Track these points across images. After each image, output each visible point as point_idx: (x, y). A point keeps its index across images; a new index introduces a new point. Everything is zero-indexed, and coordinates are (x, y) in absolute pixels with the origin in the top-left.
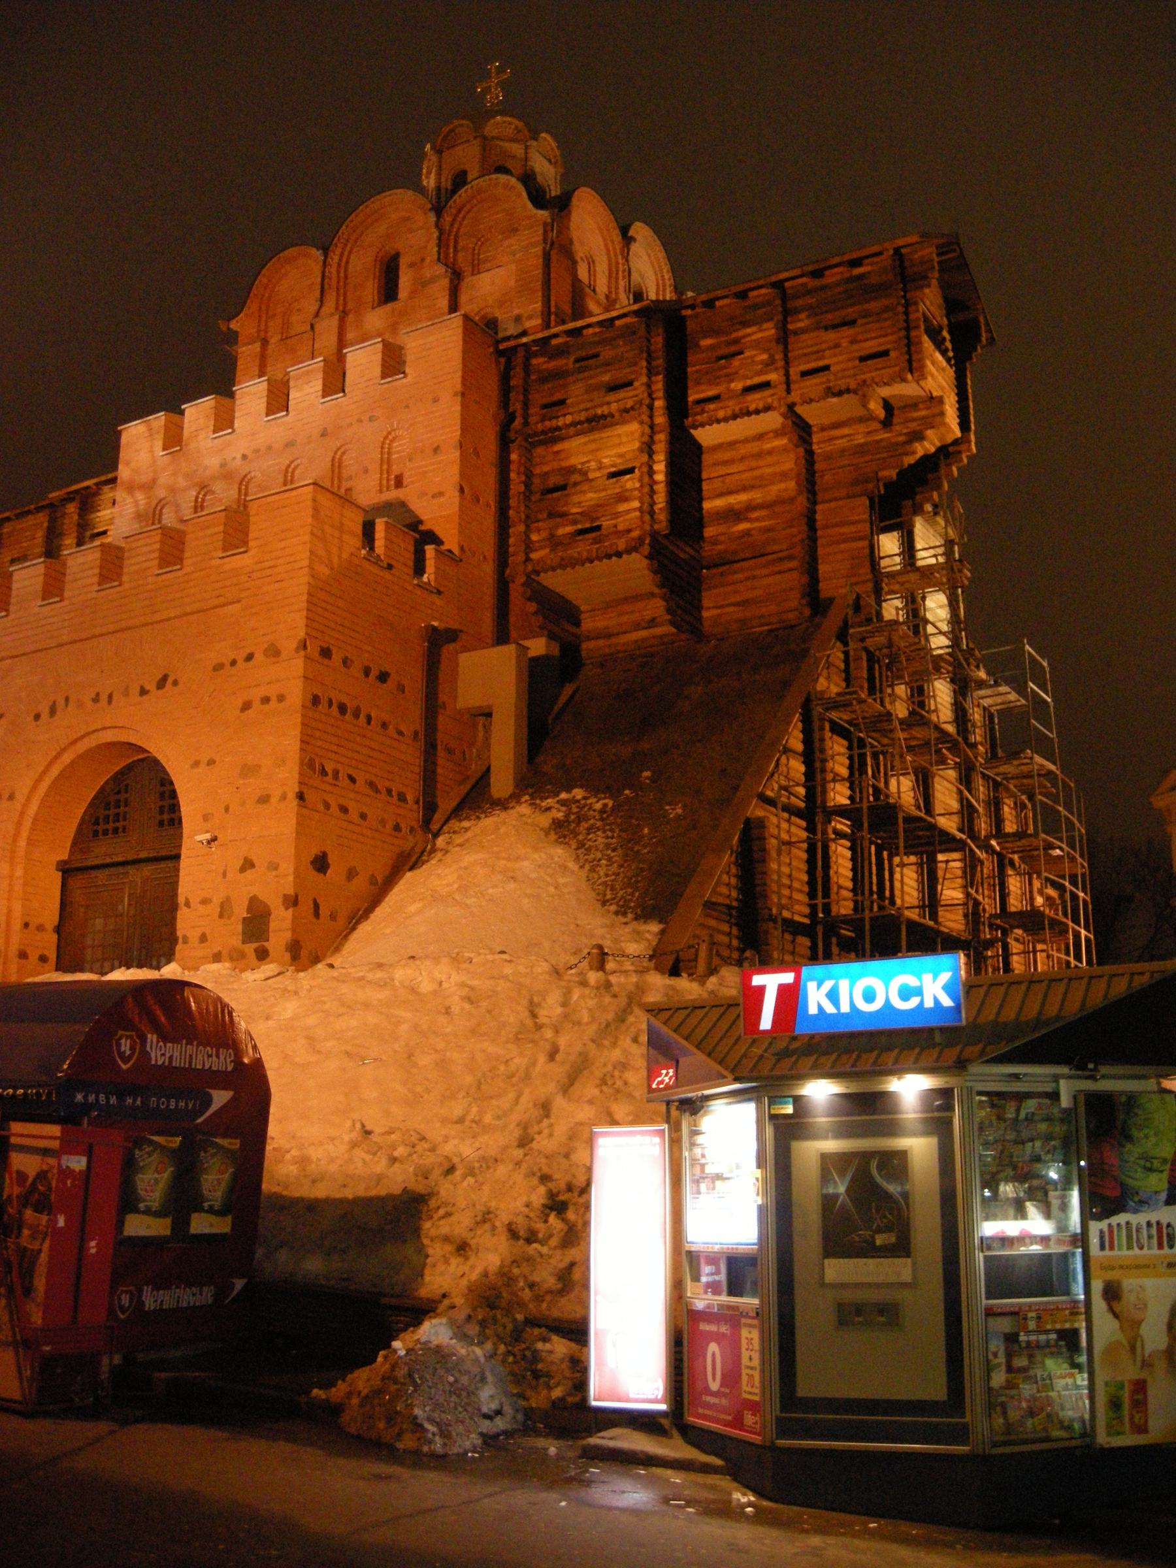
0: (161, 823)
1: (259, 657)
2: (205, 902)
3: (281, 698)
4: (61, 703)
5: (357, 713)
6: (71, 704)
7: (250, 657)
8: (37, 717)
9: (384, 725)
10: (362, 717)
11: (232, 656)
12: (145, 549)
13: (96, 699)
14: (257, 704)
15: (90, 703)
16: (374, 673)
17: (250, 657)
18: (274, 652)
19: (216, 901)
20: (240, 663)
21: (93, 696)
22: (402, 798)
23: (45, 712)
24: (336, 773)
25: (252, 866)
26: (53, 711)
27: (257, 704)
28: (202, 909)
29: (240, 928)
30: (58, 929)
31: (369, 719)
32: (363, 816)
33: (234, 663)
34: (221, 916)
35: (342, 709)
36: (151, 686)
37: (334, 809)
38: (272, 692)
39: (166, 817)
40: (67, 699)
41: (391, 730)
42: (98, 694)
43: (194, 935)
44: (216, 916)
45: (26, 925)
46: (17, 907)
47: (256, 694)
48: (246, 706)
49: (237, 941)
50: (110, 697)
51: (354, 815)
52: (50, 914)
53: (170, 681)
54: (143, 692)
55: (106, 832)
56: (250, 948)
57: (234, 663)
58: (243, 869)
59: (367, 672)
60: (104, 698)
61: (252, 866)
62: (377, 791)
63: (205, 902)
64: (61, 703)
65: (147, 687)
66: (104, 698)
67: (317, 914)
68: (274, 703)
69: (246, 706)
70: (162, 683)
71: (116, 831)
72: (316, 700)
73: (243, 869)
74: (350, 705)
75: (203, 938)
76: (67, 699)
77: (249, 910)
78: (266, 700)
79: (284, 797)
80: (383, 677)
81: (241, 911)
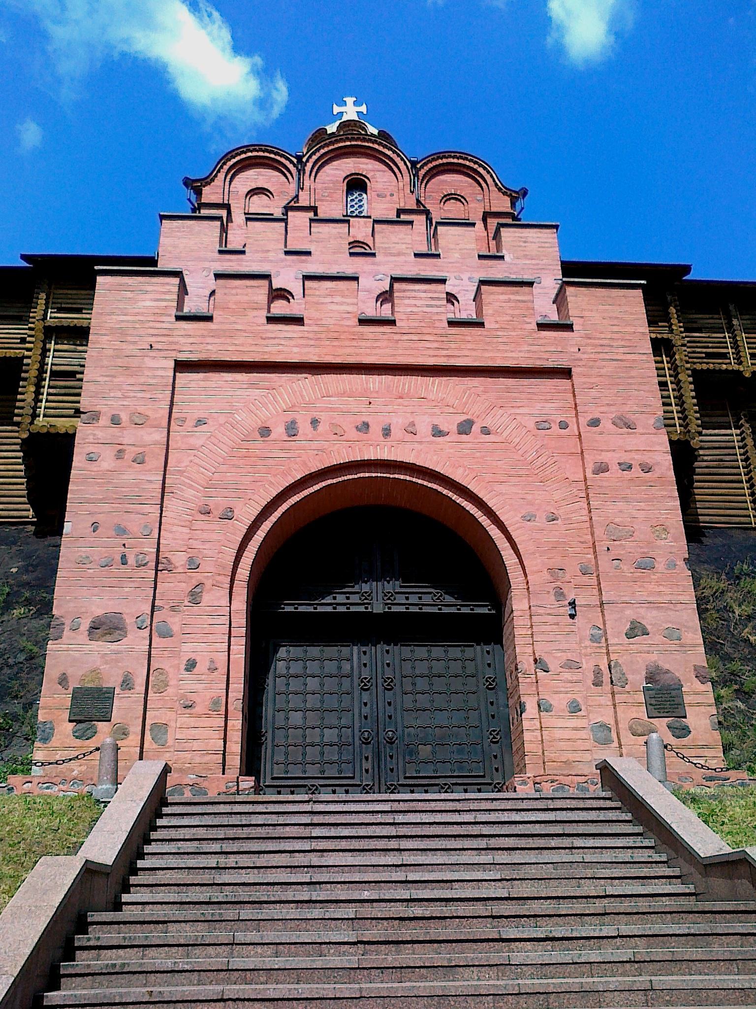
1: (606, 424)
2: (572, 665)
6: (320, 428)
8: (265, 432)
12: (423, 295)
14: (614, 467)
15: (353, 434)
17: (595, 423)
19: (588, 665)
21: (359, 424)
23: (279, 431)
25: (646, 633)
26: (292, 429)
27: (614, 467)
28: (567, 675)
38: (636, 459)
40: (315, 422)
42: (366, 425)
43: (559, 702)
44: (590, 683)
50: (387, 432)
53: (476, 428)
56: (661, 724)
60: (376, 430)
63: (572, 665)
64: (304, 427)
65: (444, 428)
66: (376, 430)
68: (636, 472)
69: (601, 469)
70: (465, 428)
75: (575, 708)
76: (315, 422)
77: (650, 679)
79: (672, 565)
81: (638, 679)
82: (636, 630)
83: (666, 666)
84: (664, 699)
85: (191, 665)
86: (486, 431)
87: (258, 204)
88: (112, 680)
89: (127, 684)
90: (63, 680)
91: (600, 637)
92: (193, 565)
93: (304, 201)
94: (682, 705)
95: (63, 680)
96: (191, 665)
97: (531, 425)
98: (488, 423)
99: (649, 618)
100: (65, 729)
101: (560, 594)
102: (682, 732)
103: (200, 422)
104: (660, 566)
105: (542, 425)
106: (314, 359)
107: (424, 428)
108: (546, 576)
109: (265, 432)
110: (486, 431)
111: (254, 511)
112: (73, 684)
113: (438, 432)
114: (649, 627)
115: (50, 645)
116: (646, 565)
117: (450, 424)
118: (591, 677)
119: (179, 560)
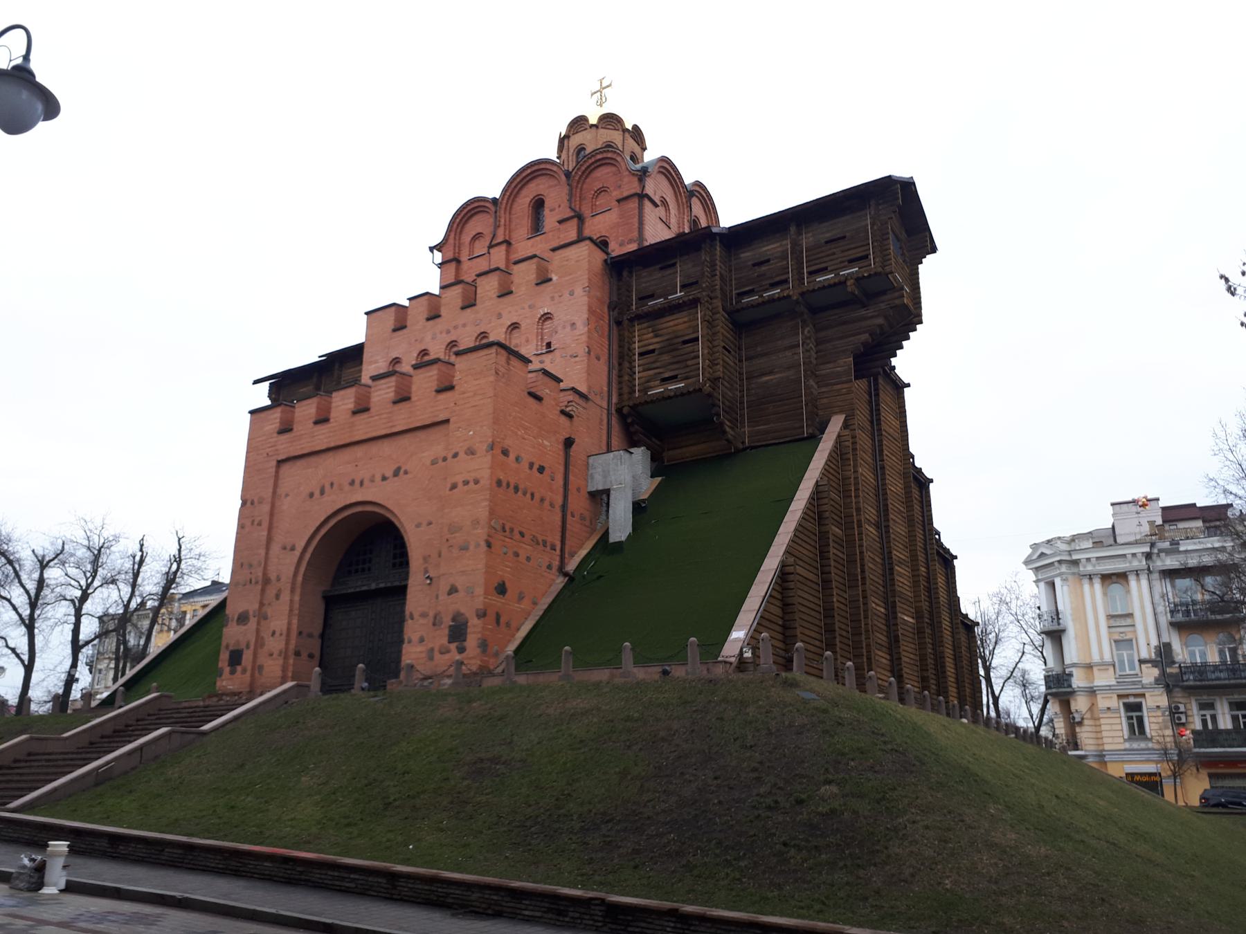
0: (394, 565)
1: (462, 455)
2: (424, 615)
3: (476, 482)
4: (327, 486)
5: (525, 494)
7: (456, 455)
8: (311, 495)
9: (542, 500)
10: (528, 495)
11: (443, 454)
13: (352, 483)
14: (460, 485)
15: (347, 487)
16: (536, 467)
17: (456, 455)
18: (471, 452)
19: (432, 614)
20: (449, 459)
22: (553, 548)
23: (317, 493)
24: (512, 530)
25: (457, 591)
26: (322, 492)
28: (422, 621)
29: (447, 632)
30: (322, 636)
31: (532, 495)
32: (528, 559)
33: (445, 459)
34: (434, 624)
35: (516, 489)
36: (389, 473)
37: (510, 554)
38: (470, 477)
39: (397, 561)
40: (332, 484)
41: (547, 503)
45: (300, 633)
46: (295, 621)
47: (459, 479)
48: (454, 487)
49: (445, 640)
50: (362, 483)
51: (522, 558)
52: (317, 628)
54: (384, 478)
55: (357, 571)
56: (453, 646)
57: (445, 459)
58: (450, 593)
59: (531, 465)
60: (357, 482)
61: (457, 591)
62: (538, 543)
63: (424, 615)
64: (327, 486)
66: (357, 482)
67: (498, 622)
69: (454, 487)
70: (396, 473)
71: (363, 570)
72: (499, 483)
73: (450, 593)
74: (521, 486)
75: (422, 640)
76: (332, 484)
77: (453, 619)
78: (466, 483)
79: (478, 545)
80: (541, 470)
81: (447, 621)
82: (453, 590)
83: (462, 611)
84: (458, 632)
85: (274, 633)
86: (406, 473)
87: (480, 247)
88: (243, 646)
89: (248, 647)
90: (227, 647)
91: (437, 597)
92: (278, 579)
93: (500, 239)
94: (466, 634)
95: (227, 647)
96: (274, 633)
97: (428, 463)
98: (407, 467)
99: (460, 582)
100: (227, 669)
101: (426, 571)
102: (461, 650)
103: (287, 495)
104: (472, 548)
105: (434, 463)
106: (332, 445)
107: (378, 478)
108: (421, 561)
109: (311, 495)
110: (406, 473)
111: (303, 544)
112: (231, 648)
113: (384, 478)
114: (459, 587)
115: (225, 630)
116: (464, 548)
117: (389, 473)
118: (432, 620)
119: (273, 577)
